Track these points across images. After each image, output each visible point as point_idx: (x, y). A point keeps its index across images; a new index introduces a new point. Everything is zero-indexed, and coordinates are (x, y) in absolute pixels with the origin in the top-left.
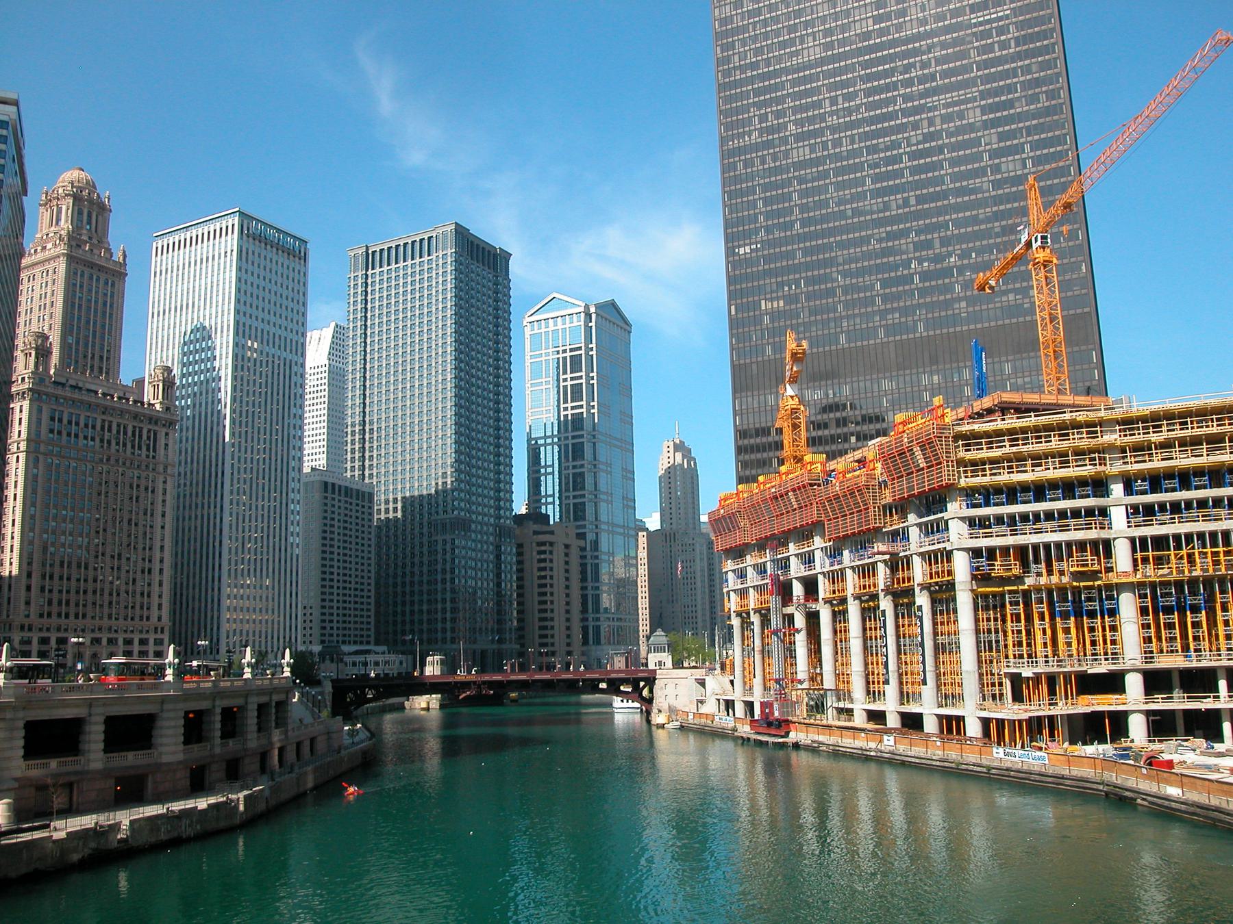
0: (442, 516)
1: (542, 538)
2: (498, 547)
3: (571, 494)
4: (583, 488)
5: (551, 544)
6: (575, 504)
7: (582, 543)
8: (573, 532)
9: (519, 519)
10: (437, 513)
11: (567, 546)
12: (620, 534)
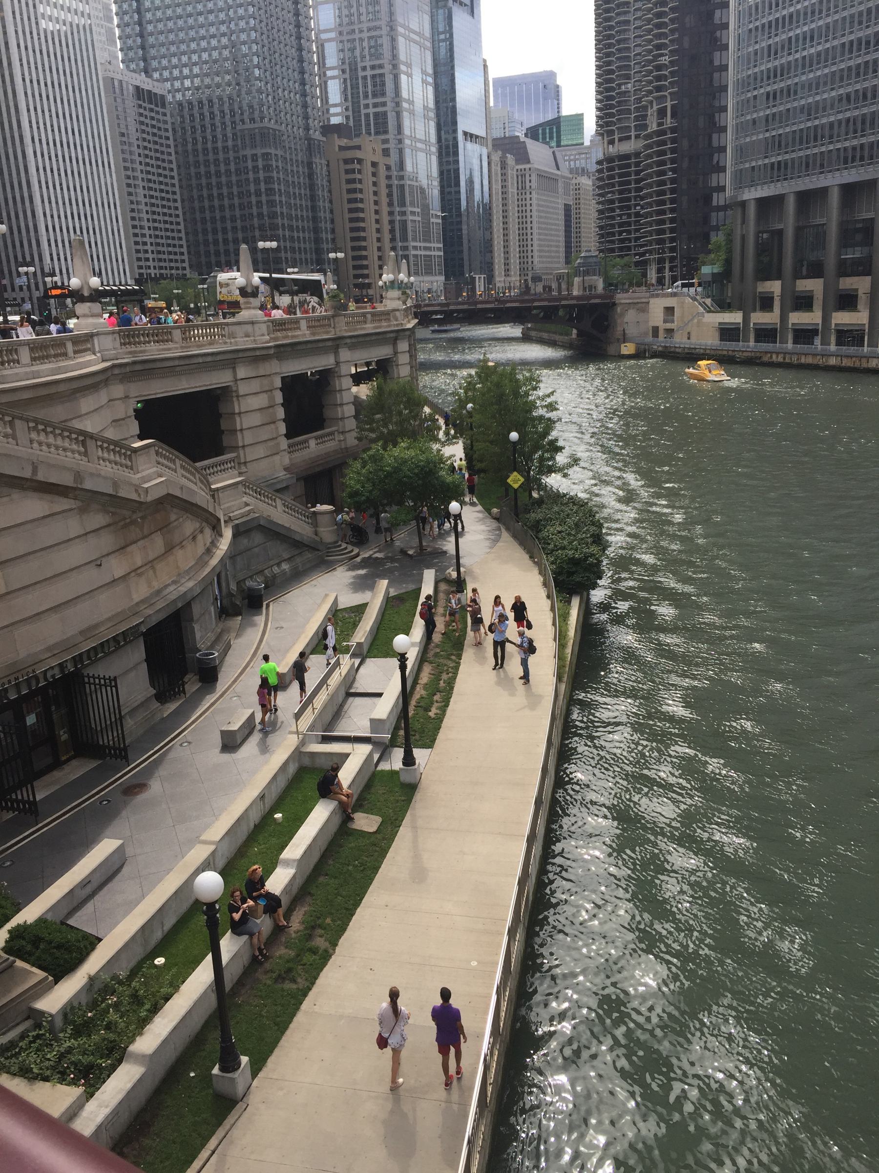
0: (248, 126)
1: (349, 154)
2: (310, 165)
4: (383, 94)
5: (360, 161)
6: (376, 115)
7: (387, 161)
8: (379, 147)
9: (328, 130)
10: (243, 121)
11: (374, 164)
12: (421, 150)
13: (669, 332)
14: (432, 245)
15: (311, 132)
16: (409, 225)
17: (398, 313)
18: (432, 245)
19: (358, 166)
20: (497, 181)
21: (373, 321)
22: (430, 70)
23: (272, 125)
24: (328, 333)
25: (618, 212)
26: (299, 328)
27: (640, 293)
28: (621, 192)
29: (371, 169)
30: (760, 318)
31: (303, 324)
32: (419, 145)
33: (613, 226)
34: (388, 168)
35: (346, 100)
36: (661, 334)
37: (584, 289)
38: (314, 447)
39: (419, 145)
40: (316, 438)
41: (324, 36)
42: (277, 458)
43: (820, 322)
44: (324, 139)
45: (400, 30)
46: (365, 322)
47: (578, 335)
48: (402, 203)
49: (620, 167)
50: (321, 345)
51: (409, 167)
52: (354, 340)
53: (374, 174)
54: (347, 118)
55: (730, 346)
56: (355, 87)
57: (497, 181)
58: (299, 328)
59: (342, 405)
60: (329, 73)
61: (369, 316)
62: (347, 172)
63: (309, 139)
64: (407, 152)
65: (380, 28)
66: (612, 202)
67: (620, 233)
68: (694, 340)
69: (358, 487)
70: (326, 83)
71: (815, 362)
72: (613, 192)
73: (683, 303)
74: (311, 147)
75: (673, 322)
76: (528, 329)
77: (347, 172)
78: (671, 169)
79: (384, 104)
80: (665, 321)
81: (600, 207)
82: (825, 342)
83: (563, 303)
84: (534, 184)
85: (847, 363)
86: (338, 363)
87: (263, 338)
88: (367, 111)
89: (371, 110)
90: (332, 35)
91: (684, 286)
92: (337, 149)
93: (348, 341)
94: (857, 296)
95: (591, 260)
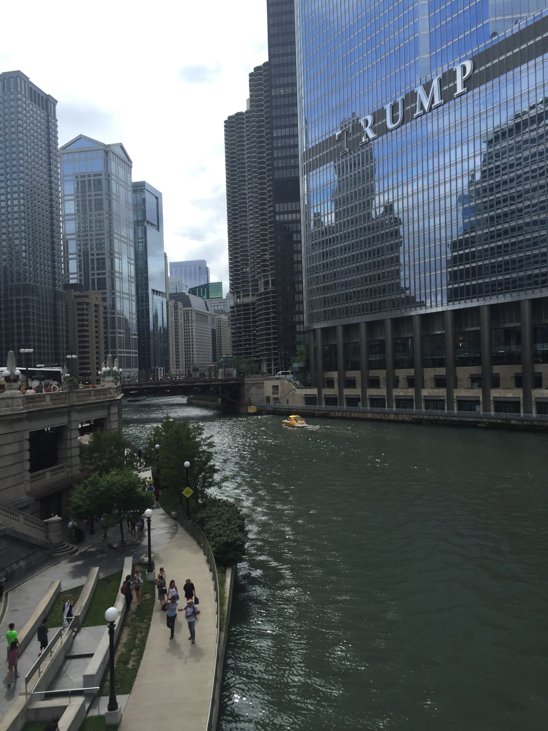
2: (55, 305)
3: (96, 272)
4: (104, 268)
5: (87, 304)
6: (98, 279)
8: (100, 297)
9: (67, 286)
11: (96, 306)
12: (126, 299)
13: (276, 399)
14: (131, 351)
15: (57, 287)
16: (117, 339)
17: (111, 390)
18: (131, 351)
19: (86, 307)
20: (172, 316)
21: (95, 395)
22: (133, 257)
23: (32, 283)
24: (64, 403)
25: (243, 333)
26: (45, 401)
27: (258, 378)
28: (245, 323)
29: (94, 308)
30: (327, 392)
31: (48, 398)
32: (124, 296)
33: (241, 341)
34: (105, 308)
35: (80, 270)
36: (271, 400)
37: (225, 375)
38: (49, 477)
39: (124, 296)
40: (51, 471)
41: (68, 237)
42: (22, 485)
43: (360, 394)
44: (65, 291)
45: (115, 235)
46: (90, 396)
47: (222, 402)
48: (113, 327)
49: (244, 310)
50: (58, 411)
51: (118, 307)
52: (81, 407)
53: (96, 311)
54: (81, 280)
55: (311, 407)
56: (86, 264)
57: (172, 316)
58: (45, 401)
59: (71, 448)
60: (70, 257)
61: (93, 392)
62: (79, 310)
63: (55, 292)
64: (118, 299)
65: (103, 234)
66: (240, 328)
67: (245, 345)
68: (290, 404)
69: (81, 502)
70: (68, 262)
71: (360, 416)
72: (240, 323)
73: (284, 383)
74: (56, 295)
75: (278, 394)
76: (191, 398)
77: (79, 310)
78: (272, 312)
79: (104, 274)
80: (273, 394)
81: (233, 331)
82: (364, 405)
83: (212, 383)
84: (194, 318)
85: (377, 416)
86: (70, 422)
87: (20, 408)
88: (93, 277)
89: (96, 277)
90: (74, 237)
91: (283, 374)
92: (73, 297)
93: (78, 408)
94: (379, 380)
95: (229, 359)
